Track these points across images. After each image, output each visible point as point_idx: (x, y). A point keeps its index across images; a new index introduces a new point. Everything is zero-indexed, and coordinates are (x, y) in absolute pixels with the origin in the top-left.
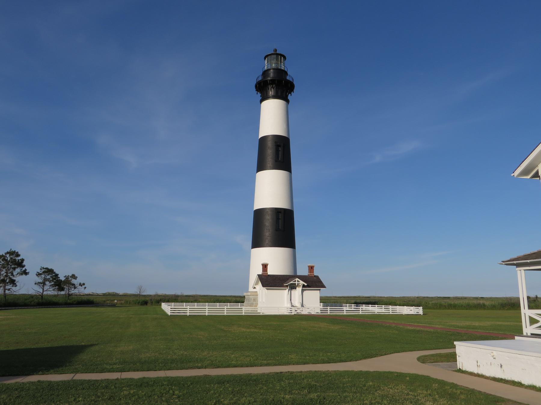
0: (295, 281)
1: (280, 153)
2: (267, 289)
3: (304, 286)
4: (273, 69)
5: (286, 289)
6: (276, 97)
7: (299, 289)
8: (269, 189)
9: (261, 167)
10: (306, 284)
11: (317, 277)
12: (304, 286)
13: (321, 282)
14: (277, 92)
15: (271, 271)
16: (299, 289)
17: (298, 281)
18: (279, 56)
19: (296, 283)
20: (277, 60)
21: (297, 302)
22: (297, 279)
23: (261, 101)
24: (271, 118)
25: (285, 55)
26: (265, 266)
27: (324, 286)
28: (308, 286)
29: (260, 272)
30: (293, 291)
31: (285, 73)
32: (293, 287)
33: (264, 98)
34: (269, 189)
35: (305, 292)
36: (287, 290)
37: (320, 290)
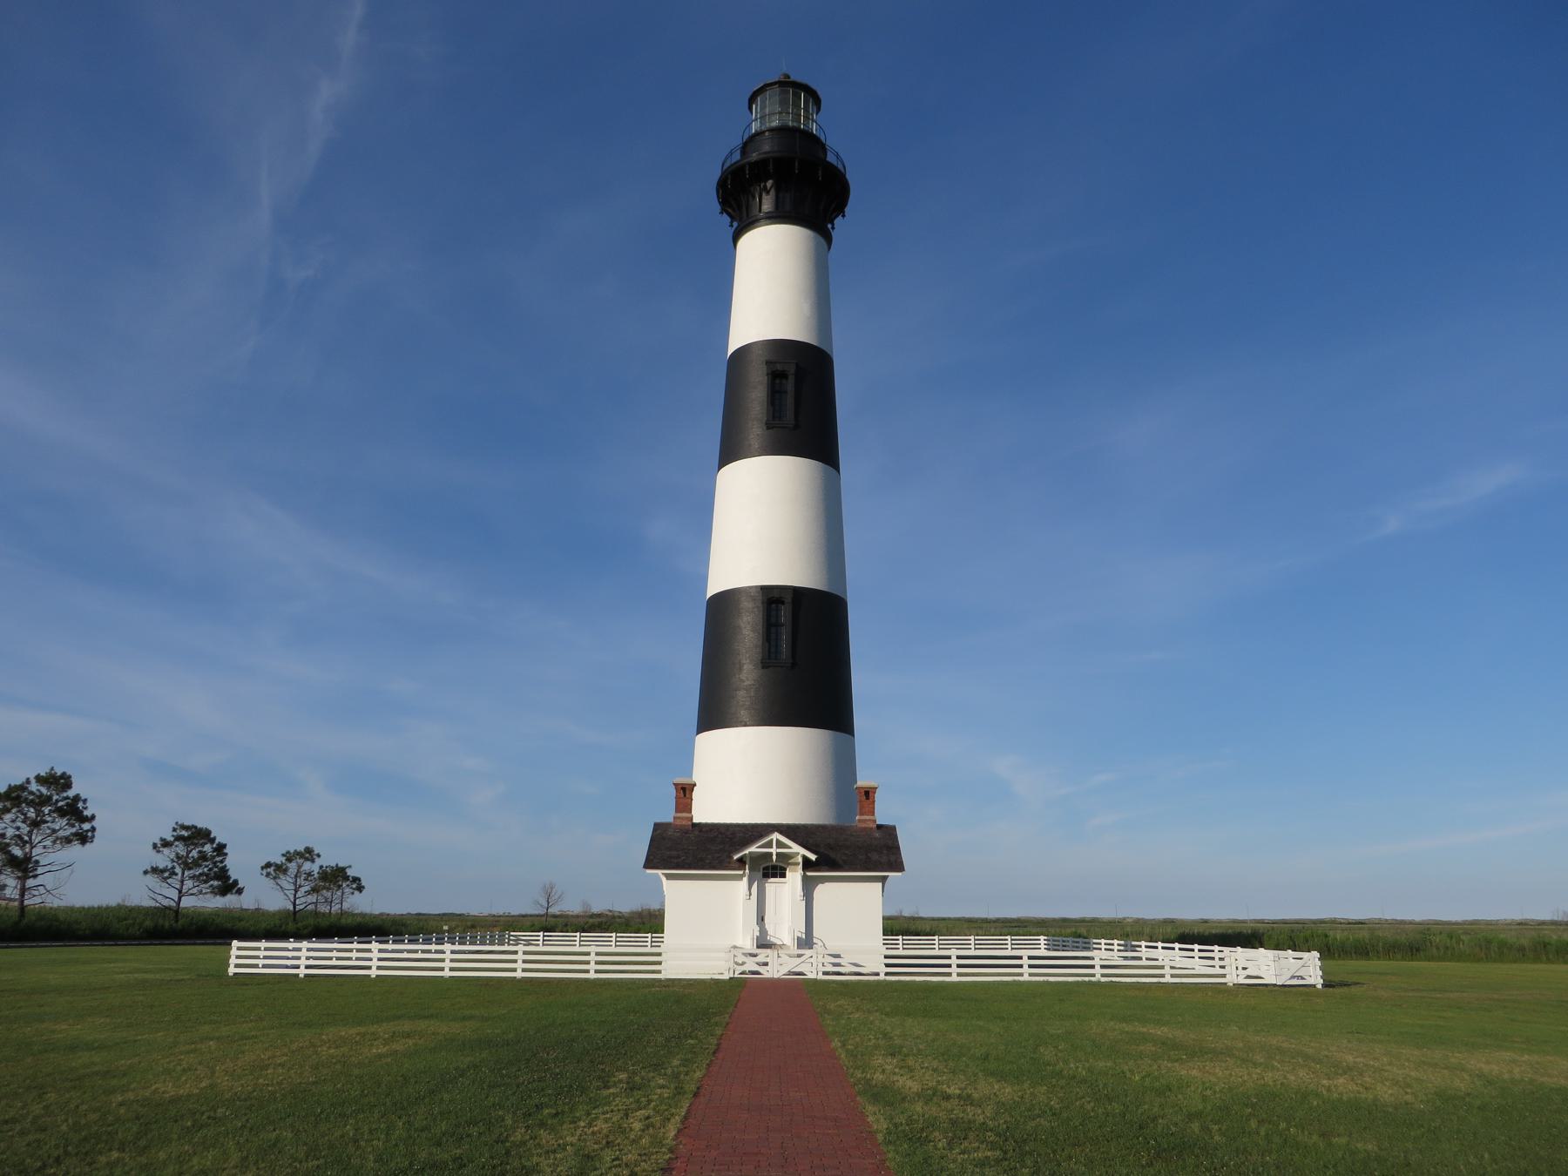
0: (769, 845)
1: (790, 400)
2: (669, 877)
3: (807, 864)
4: (771, 130)
5: (740, 878)
6: (778, 216)
7: (794, 877)
8: (757, 521)
9: (730, 452)
10: (813, 857)
11: (889, 832)
12: (807, 864)
13: (895, 849)
14: (778, 203)
15: (706, 811)
16: (794, 877)
17: (780, 844)
18: (792, 88)
19: (774, 850)
20: (784, 103)
21: (785, 928)
22: (776, 836)
23: (736, 237)
24: (767, 284)
25: (814, 87)
26: (685, 792)
27: (898, 866)
28: (834, 866)
29: (668, 815)
30: (772, 885)
32: (773, 869)
33: (744, 222)
34: (757, 521)
35: (823, 892)
36: (745, 879)
37: (883, 880)
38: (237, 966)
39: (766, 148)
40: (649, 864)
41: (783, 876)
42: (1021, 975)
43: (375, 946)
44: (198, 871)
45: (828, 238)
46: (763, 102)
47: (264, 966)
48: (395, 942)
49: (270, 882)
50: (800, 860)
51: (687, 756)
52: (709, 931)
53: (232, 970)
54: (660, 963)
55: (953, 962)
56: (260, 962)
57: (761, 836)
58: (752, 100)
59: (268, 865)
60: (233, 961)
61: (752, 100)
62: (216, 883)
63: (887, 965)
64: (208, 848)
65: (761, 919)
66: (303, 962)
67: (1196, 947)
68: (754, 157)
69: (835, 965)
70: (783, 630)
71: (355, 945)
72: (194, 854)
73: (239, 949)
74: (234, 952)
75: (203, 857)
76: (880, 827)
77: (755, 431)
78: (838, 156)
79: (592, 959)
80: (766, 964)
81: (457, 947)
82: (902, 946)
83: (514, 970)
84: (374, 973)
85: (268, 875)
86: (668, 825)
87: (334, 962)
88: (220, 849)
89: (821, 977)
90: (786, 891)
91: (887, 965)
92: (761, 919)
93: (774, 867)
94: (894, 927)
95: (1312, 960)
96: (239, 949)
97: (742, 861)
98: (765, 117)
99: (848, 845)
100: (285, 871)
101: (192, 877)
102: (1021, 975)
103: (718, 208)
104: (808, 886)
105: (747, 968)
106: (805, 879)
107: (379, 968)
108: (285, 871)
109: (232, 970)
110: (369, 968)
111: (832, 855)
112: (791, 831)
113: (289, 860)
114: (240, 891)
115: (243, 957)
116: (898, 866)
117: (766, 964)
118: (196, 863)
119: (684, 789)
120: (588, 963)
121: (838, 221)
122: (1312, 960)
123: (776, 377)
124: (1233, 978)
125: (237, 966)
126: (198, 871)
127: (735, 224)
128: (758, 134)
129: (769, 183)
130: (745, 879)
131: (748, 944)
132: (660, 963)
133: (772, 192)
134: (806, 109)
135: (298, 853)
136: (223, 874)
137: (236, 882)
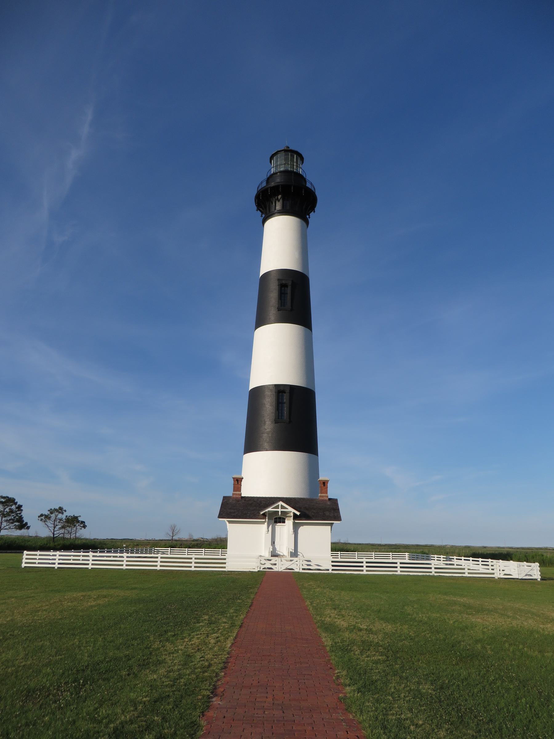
0: (277, 507)
1: (289, 297)
3: (295, 517)
4: (281, 172)
5: (263, 523)
6: (284, 212)
7: (289, 522)
8: (272, 355)
9: (260, 322)
10: (298, 513)
11: (334, 502)
12: (295, 517)
14: (283, 206)
15: (247, 491)
16: (289, 522)
17: (283, 507)
18: (292, 153)
19: (280, 510)
20: (286, 159)
22: (281, 503)
23: (264, 222)
26: (238, 481)
27: (338, 518)
28: (308, 517)
29: (230, 493)
30: (279, 526)
31: (300, 178)
32: (279, 519)
34: (272, 355)
35: (302, 530)
36: (266, 524)
37: (331, 524)
38: (26, 563)
39: (278, 180)
40: (221, 516)
41: (284, 522)
42: (396, 571)
43: (91, 554)
44: (9, 518)
45: (307, 222)
46: (277, 159)
47: (39, 563)
48: (100, 552)
49: (42, 524)
50: (292, 515)
51: (239, 465)
52: (248, 548)
53: (24, 565)
54: (225, 563)
55: (365, 565)
56: (37, 561)
57: (274, 503)
58: (272, 158)
59: (42, 515)
60: (24, 561)
61: (272, 158)
62: (17, 524)
63: (333, 566)
64: (14, 507)
65: (273, 543)
66: (57, 561)
67: (480, 559)
68: (273, 184)
69: (308, 565)
70: (285, 405)
71: (82, 554)
72: (7, 510)
73: (27, 555)
74: (25, 556)
75: (12, 511)
76: (330, 499)
77: (272, 311)
78: (311, 184)
79: (193, 561)
80: (275, 564)
81: (130, 555)
82: (340, 556)
83: (156, 566)
84: (90, 567)
85: (41, 520)
86: (230, 497)
87: (72, 562)
88: (19, 507)
89: (301, 571)
90: (285, 529)
91: (333, 566)
92: (273, 543)
93: (280, 518)
94: (336, 547)
95: (536, 566)
96: (27, 555)
97: (264, 515)
98: (279, 166)
99: (315, 508)
100: (49, 518)
101: (6, 521)
102: (396, 571)
103: (256, 208)
104: (296, 527)
105: (266, 566)
106: (294, 524)
107: (92, 564)
108: (49, 518)
109: (24, 565)
110: (88, 564)
111: (307, 512)
112: (288, 501)
113: (51, 513)
114: (28, 528)
115: (30, 559)
116: (338, 518)
117: (275, 564)
118: (8, 514)
119: (237, 480)
120: (191, 563)
121: (312, 214)
122: (536, 566)
123: (282, 286)
124: (498, 575)
125: (26, 563)
126: (9, 518)
127: (263, 216)
128: (274, 174)
129: (280, 197)
130: (266, 524)
131: (267, 555)
132: (225, 563)
133: (281, 201)
134: (297, 162)
135: (56, 510)
136: (20, 520)
137: (26, 523)
